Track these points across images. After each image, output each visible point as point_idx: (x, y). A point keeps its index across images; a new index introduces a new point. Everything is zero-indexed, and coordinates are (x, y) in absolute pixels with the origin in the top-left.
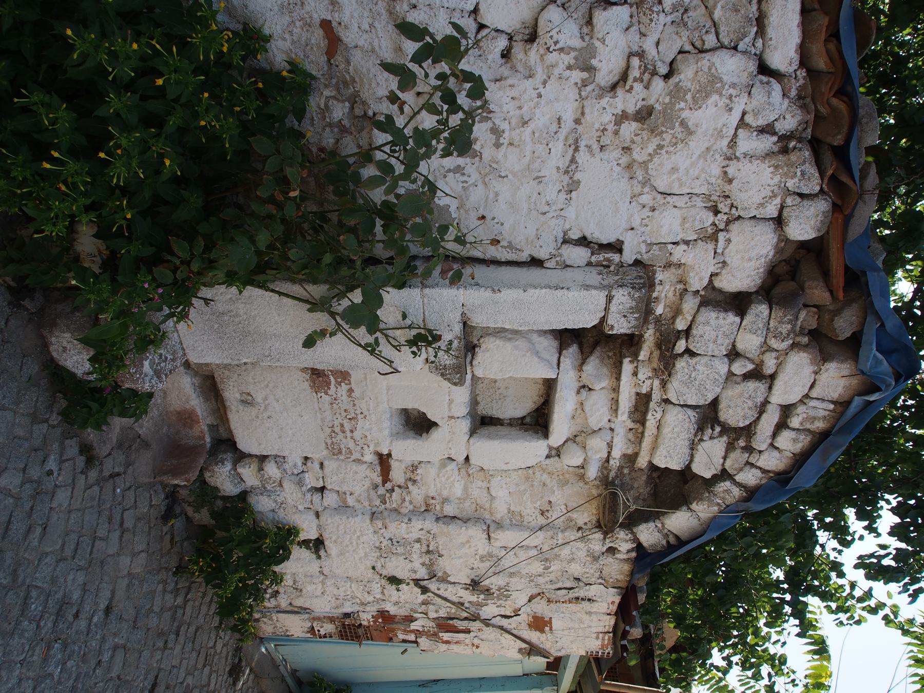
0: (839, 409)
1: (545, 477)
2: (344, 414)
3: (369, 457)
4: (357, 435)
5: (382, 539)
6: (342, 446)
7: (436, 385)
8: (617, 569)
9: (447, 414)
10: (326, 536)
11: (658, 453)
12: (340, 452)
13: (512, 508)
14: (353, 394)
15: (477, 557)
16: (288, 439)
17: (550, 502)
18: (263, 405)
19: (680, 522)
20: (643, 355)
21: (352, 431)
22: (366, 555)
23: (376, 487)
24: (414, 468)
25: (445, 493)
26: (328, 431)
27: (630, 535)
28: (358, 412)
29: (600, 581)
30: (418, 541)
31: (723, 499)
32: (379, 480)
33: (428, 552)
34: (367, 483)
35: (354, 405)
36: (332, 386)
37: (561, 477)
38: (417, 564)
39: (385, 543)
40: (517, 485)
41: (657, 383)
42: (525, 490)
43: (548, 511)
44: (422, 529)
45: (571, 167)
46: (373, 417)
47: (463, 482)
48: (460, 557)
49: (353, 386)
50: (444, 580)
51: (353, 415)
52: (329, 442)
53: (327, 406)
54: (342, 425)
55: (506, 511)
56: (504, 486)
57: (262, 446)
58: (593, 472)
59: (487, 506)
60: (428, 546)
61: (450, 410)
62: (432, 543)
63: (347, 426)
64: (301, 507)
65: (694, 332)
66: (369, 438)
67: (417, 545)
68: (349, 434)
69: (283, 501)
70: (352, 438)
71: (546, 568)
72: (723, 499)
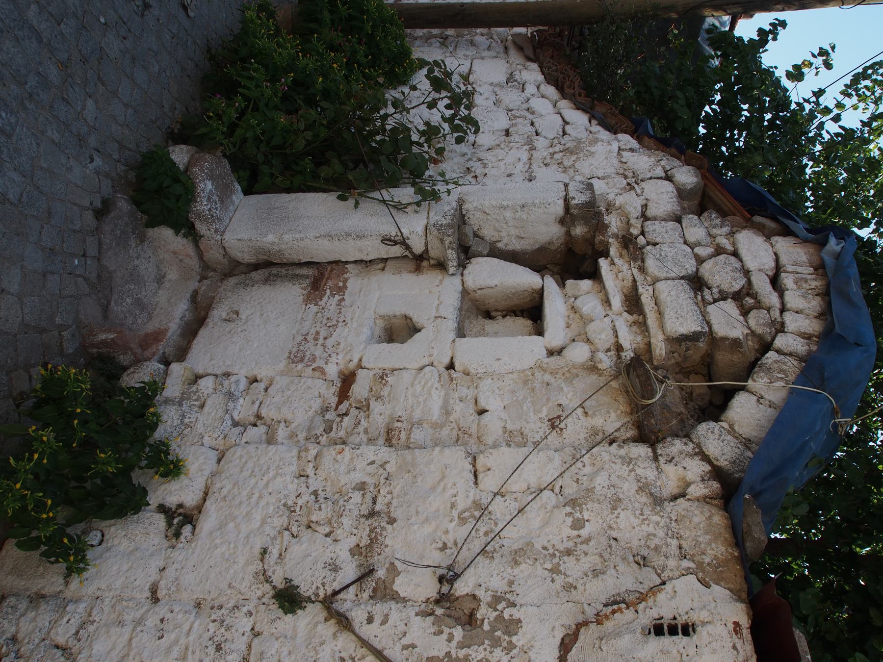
0: (820, 271)
1: (547, 377)
2: (325, 321)
3: (332, 370)
4: (330, 342)
5: (303, 489)
6: (308, 354)
7: (427, 291)
8: (702, 527)
9: (434, 314)
10: (207, 523)
11: (666, 317)
12: (302, 360)
13: (510, 427)
14: (343, 304)
15: (455, 513)
16: (248, 352)
17: (560, 405)
18: (243, 321)
19: (748, 412)
20: (613, 251)
21: (325, 338)
22: (264, 522)
23: (325, 410)
24: (382, 377)
25: (417, 415)
26: (299, 338)
27: (691, 445)
28: (341, 320)
29: (686, 564)
30: (361, 487)
31: (781, 371)
32: (334, 400)
33: (372, 514)
34: (317, 405)
35: (340, 313)
36: (325, 299)
37: (568, 375)
38: (342, 551)
39: (305, 498)
40: (513, 392)
41: (635, 271)
42: (525, 398)
43: (559, 417)
44: (373, 463)
45: (530, 170)
46: (355, 324)
47: (443, 393)
48: (427, 520)
49: (346, 297)
50: (384, 593)
51: (334, 322)
52: (294, 350)
53: (311, 316)
54: (318, 333)
55: (500, 432)
56: (497, 391)
57: (213, 362)
58: (606, 361)
59: (474, 430)
60: (374, 501)
61: (437, 310)
62: (383, 492)
63: (323, 334)
64: (206, 440)
65: (647, 230)
66: (341, 346)
67: (357, 497)
68: (321, 341)
69: (193, 426)
70: (323, 345)
71: (578, 524)
72: (781, 371)
